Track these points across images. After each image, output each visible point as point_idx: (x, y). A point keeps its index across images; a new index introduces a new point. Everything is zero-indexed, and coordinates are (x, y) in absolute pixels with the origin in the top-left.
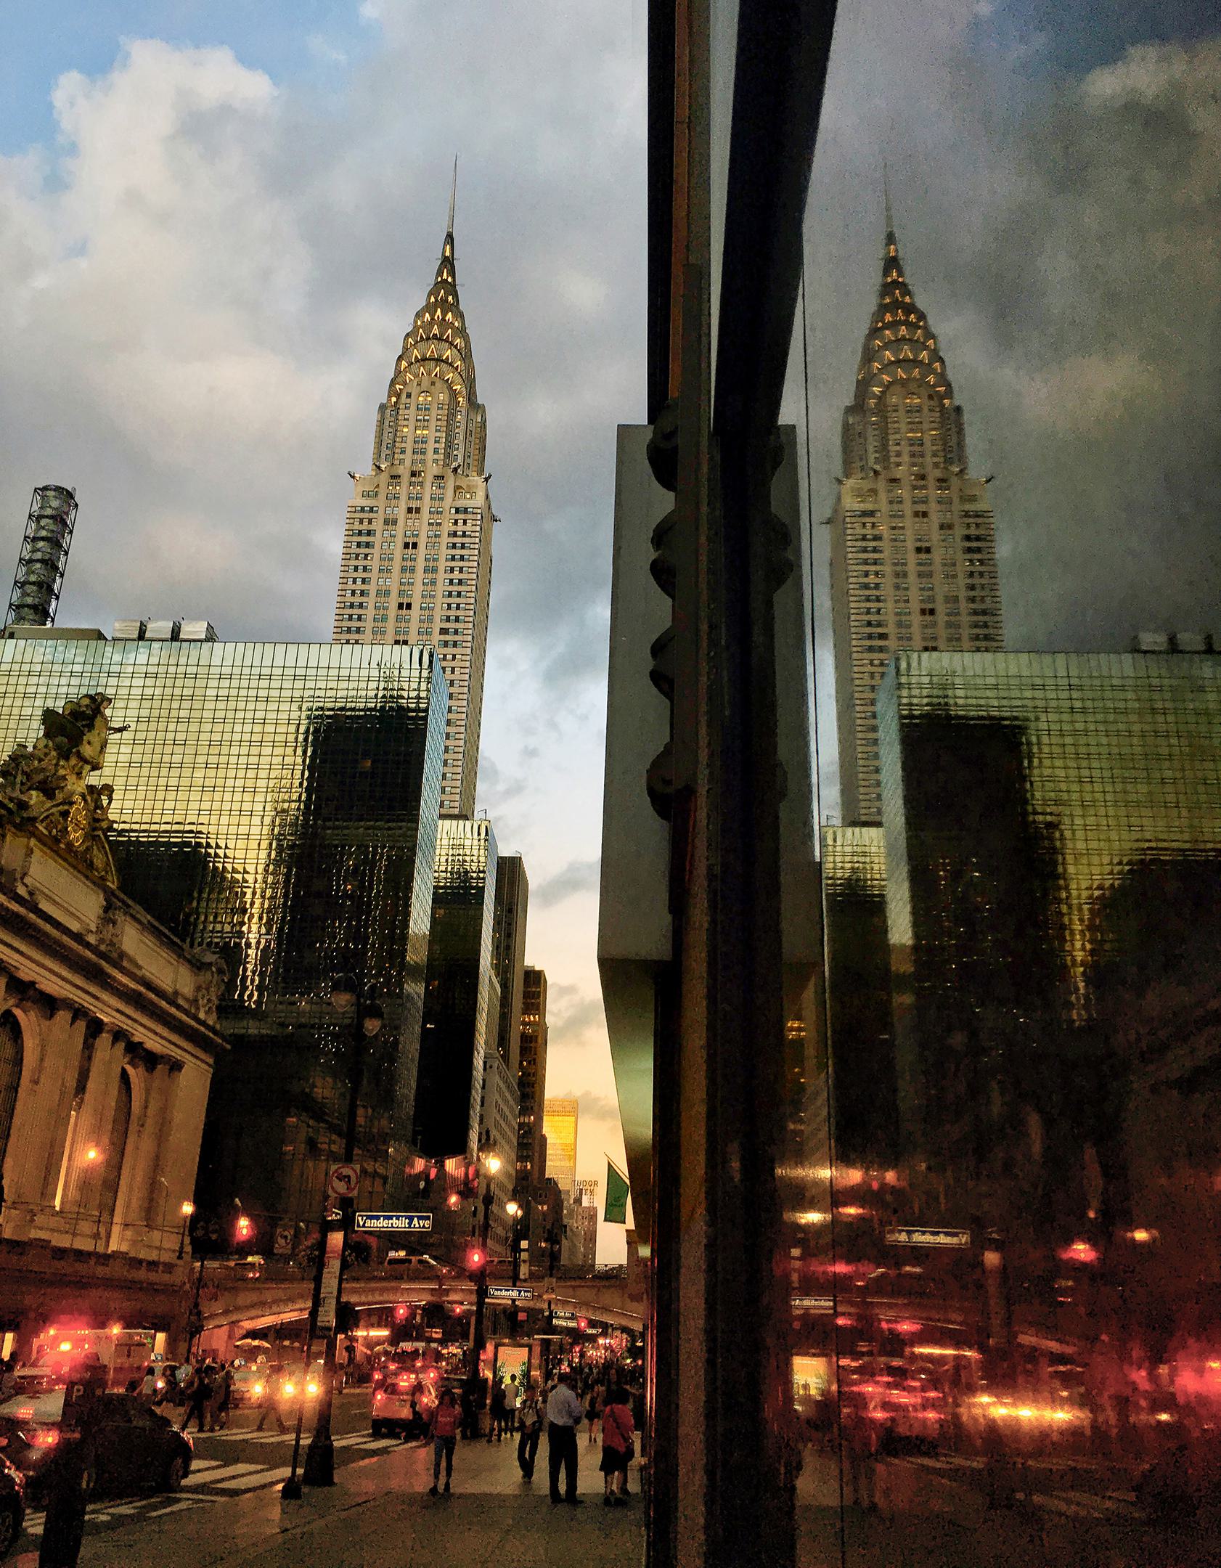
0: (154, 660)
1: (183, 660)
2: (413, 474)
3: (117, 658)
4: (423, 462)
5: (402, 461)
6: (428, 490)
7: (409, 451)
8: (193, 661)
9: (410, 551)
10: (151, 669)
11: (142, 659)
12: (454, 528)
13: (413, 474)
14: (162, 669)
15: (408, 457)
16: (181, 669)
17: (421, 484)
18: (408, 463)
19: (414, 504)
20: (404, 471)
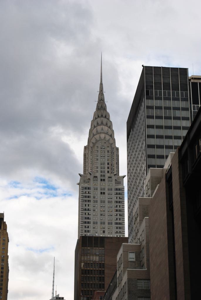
4: (104, 172)
18: (99, 172)
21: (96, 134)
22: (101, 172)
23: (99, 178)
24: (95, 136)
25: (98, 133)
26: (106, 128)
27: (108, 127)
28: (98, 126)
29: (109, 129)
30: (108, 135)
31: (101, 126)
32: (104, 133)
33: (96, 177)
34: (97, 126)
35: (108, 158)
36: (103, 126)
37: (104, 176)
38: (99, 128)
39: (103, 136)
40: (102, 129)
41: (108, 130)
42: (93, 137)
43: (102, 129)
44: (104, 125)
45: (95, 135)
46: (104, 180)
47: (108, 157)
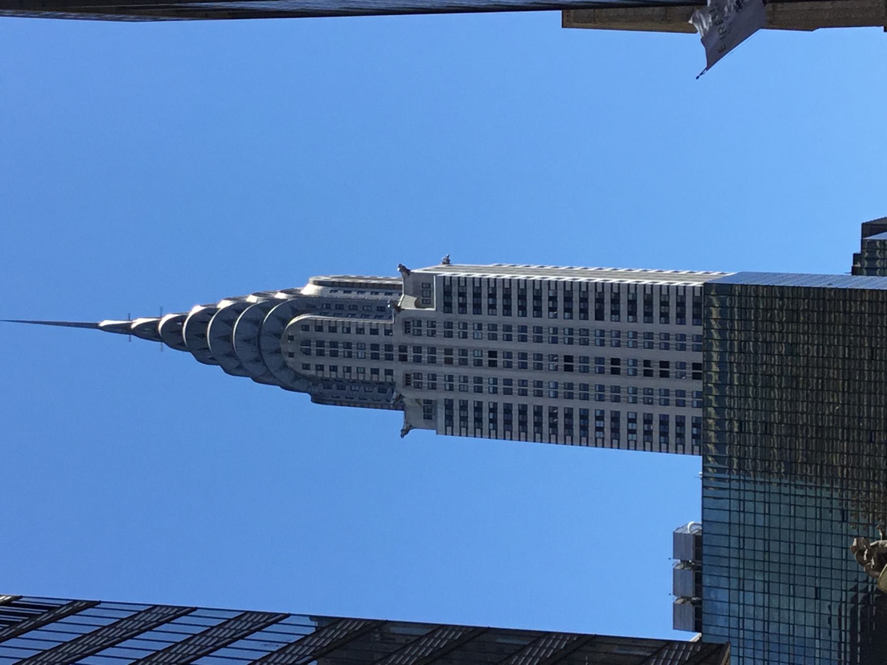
0: (724, 582)
1: (724, 552)
2: (403, 359)
3: (721, 621)
5: (389, 372)
6: (424, 341)
7: (375, 364)
8: (724, 542)
10: (734, 584)
11: (723, 595)
12: (470, 309)
13: (403, 359)
14: (733, 573)
15: (382, 365)
16: (734, 553)
18: (389, 365)
19: (440, 357)
20: (399, 370)
21: (265, 364)
22: (389, 358)
23: (410, 367)
25: (259, 360)
32: (259, 335)
33: (407, 377)
34: (238, 359)
37: (403, 348)
42: (275, 377)
46: (417, 349)
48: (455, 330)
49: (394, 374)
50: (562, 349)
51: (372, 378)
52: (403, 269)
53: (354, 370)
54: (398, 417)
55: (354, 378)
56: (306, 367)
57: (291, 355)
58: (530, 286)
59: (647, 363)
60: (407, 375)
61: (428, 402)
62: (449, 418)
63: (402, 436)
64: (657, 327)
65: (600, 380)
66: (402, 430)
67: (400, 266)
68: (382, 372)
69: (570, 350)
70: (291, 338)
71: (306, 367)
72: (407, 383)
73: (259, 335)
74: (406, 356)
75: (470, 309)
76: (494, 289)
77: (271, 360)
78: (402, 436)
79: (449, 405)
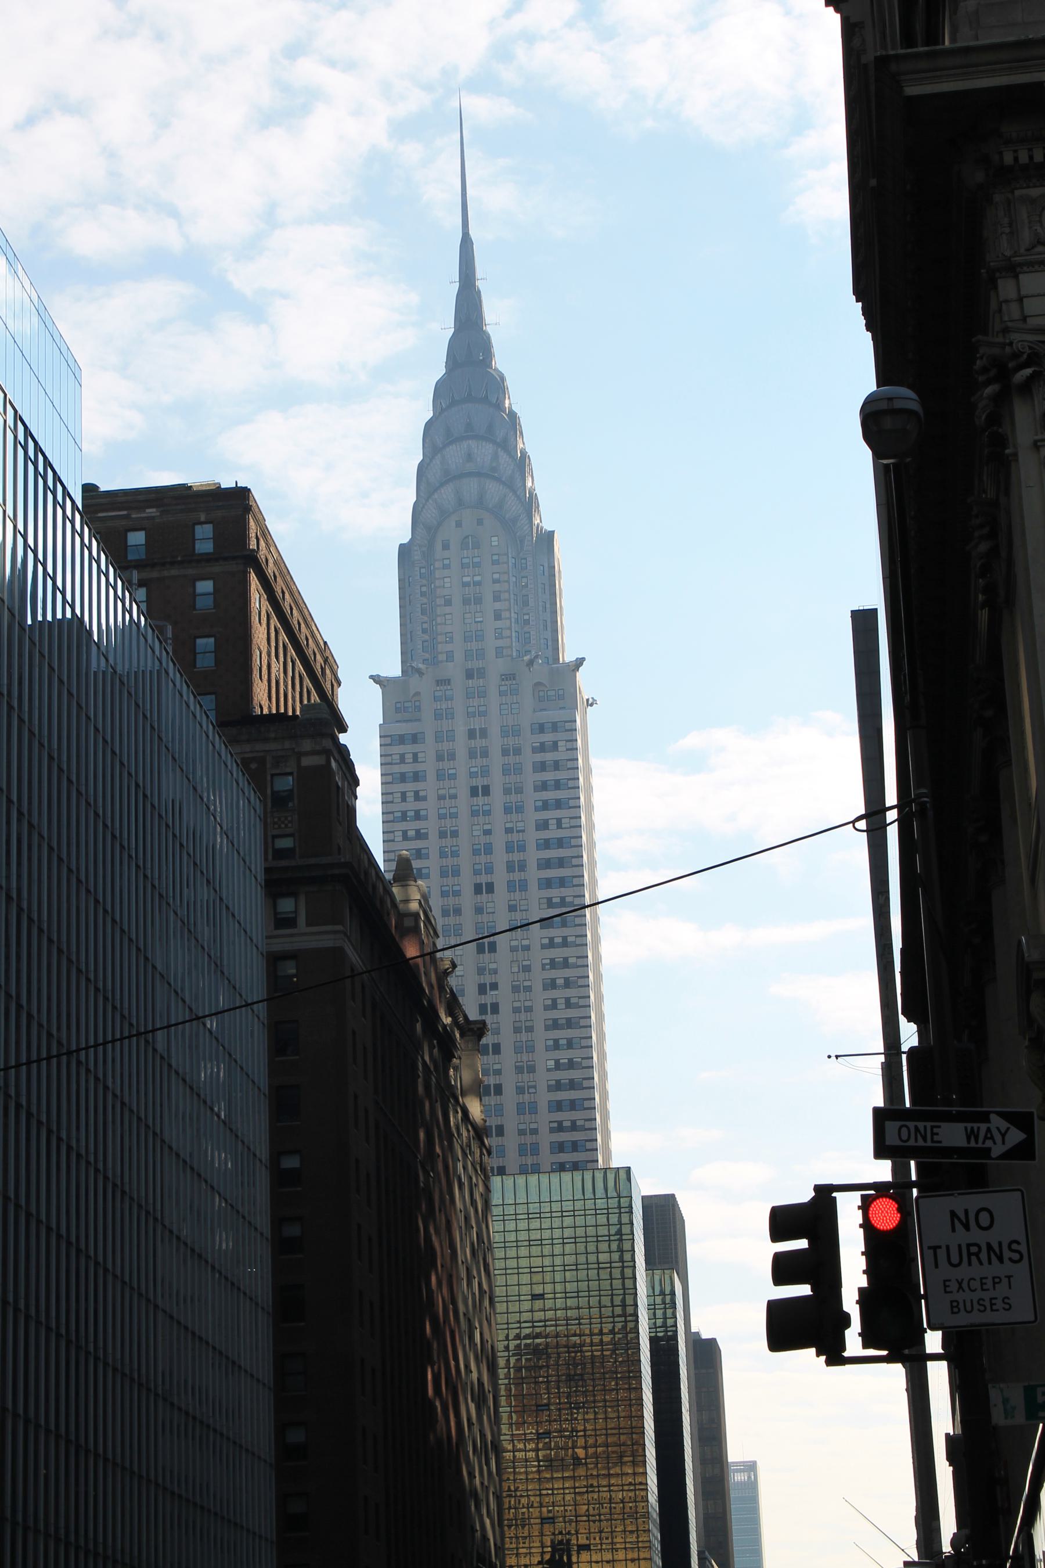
2: (469, 675)
4: (481, 654)
9: (481, 800)
12: (539, 757)
17: (483, 694)
18: (459, 656)
19: (476, 724)
20: (454, 670)
21: (442, 485)
24: (436, 496)
26: (484, 452)
27: (495, 443)
28: (451, 443)
29: (501, 453)
30: (498, 480)
31: (465, 444)
32: (478, 474)
33: (448, 682)
34: (445, 446)
35: (497, 587)
36: (473, 443)
37: (481, 673)
38: (454, 455)
39: (470, 488)
40: (469, 457)
41: (495, 456)
42: (427, 500)
43: (469, 457)
44: (476, 437)
45: (435, 490)
47: (495, 581)
48: (511, 759)
49: (451, 664)
50: (500, 878)
51: (441, 634)
52: (580, 662)
53: (447, 609)
54: (393, 669)
55: (439, 611)
56: (446, 546)
57: (459, 524)
58: (579, 972)
59: (494, 986)
60: (449, 680)
61: (418, 709)
62: (401, 740)
63: (371, 677)
64: (542, 1037)
65: (466, 871)
66: (378, 676)
67: (583, 659)
68: (449, 647)
69: (497, 790)
70: (480, 522)
71: (446, 546)
72: (439, 682)
73: (478, 474)
74: (472, 678)
75: (539, 757)
76: (578, 1006)
77: (447, 494)
78: (371, 677)
79: (415, 739)
